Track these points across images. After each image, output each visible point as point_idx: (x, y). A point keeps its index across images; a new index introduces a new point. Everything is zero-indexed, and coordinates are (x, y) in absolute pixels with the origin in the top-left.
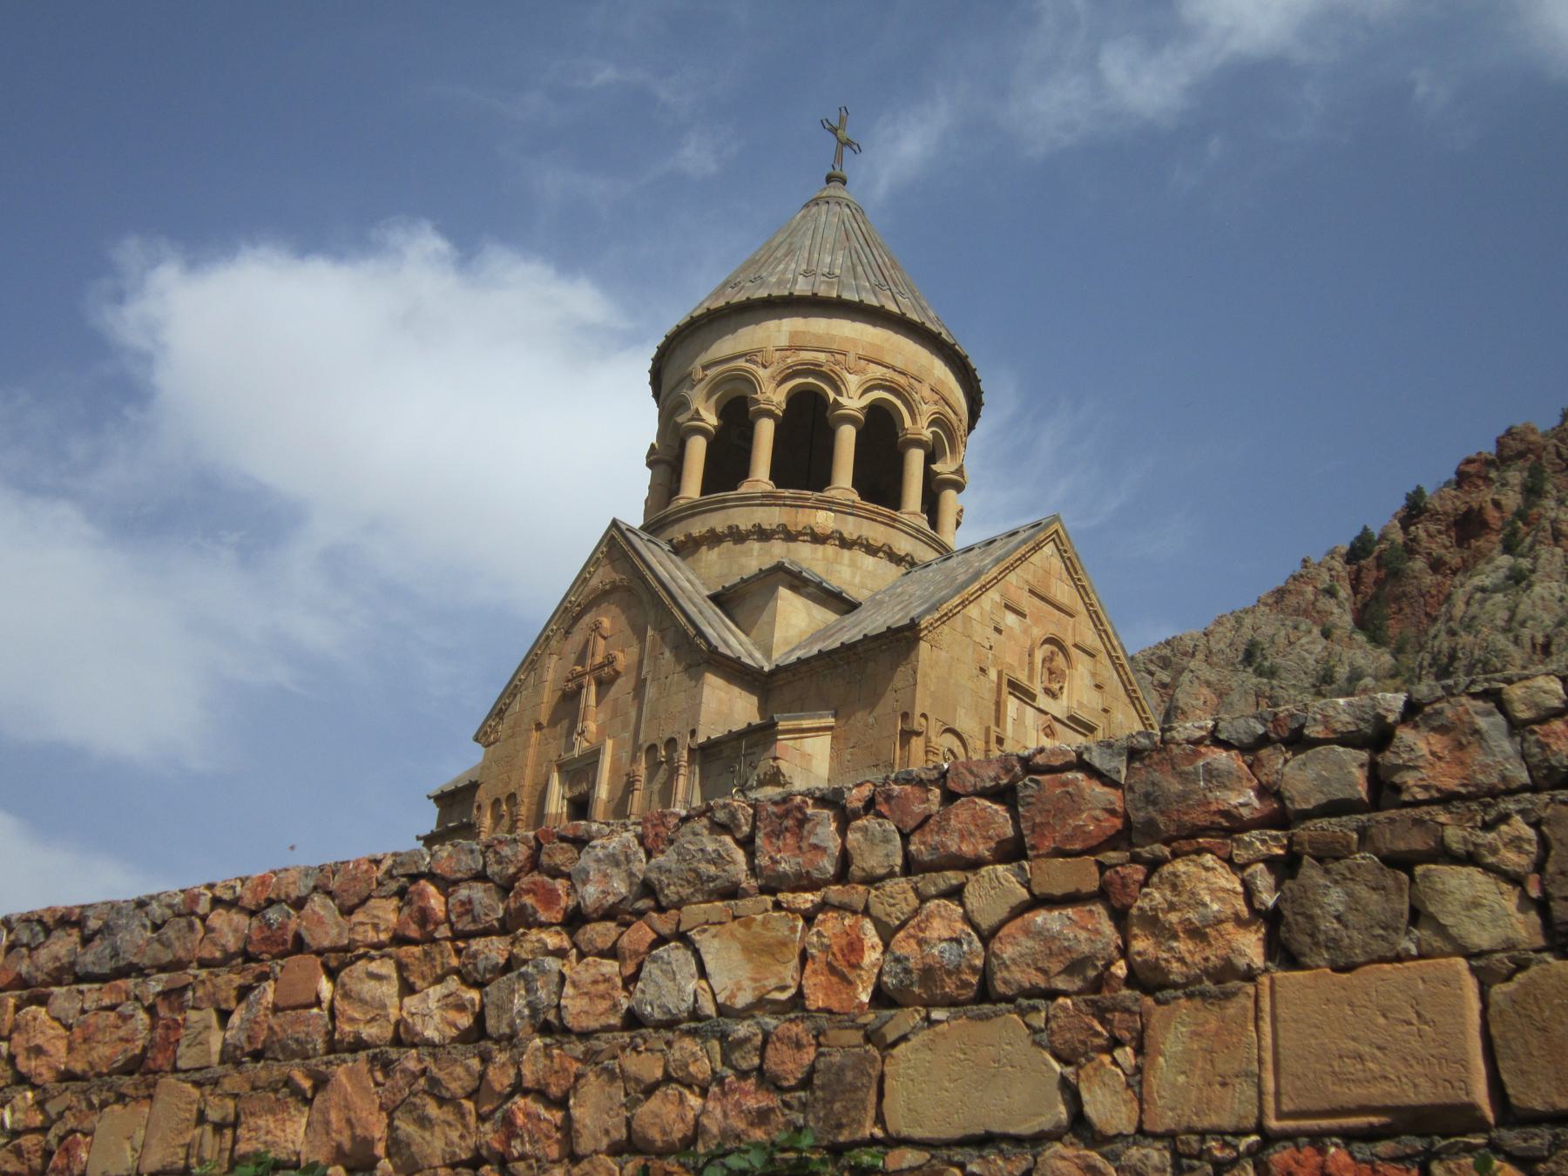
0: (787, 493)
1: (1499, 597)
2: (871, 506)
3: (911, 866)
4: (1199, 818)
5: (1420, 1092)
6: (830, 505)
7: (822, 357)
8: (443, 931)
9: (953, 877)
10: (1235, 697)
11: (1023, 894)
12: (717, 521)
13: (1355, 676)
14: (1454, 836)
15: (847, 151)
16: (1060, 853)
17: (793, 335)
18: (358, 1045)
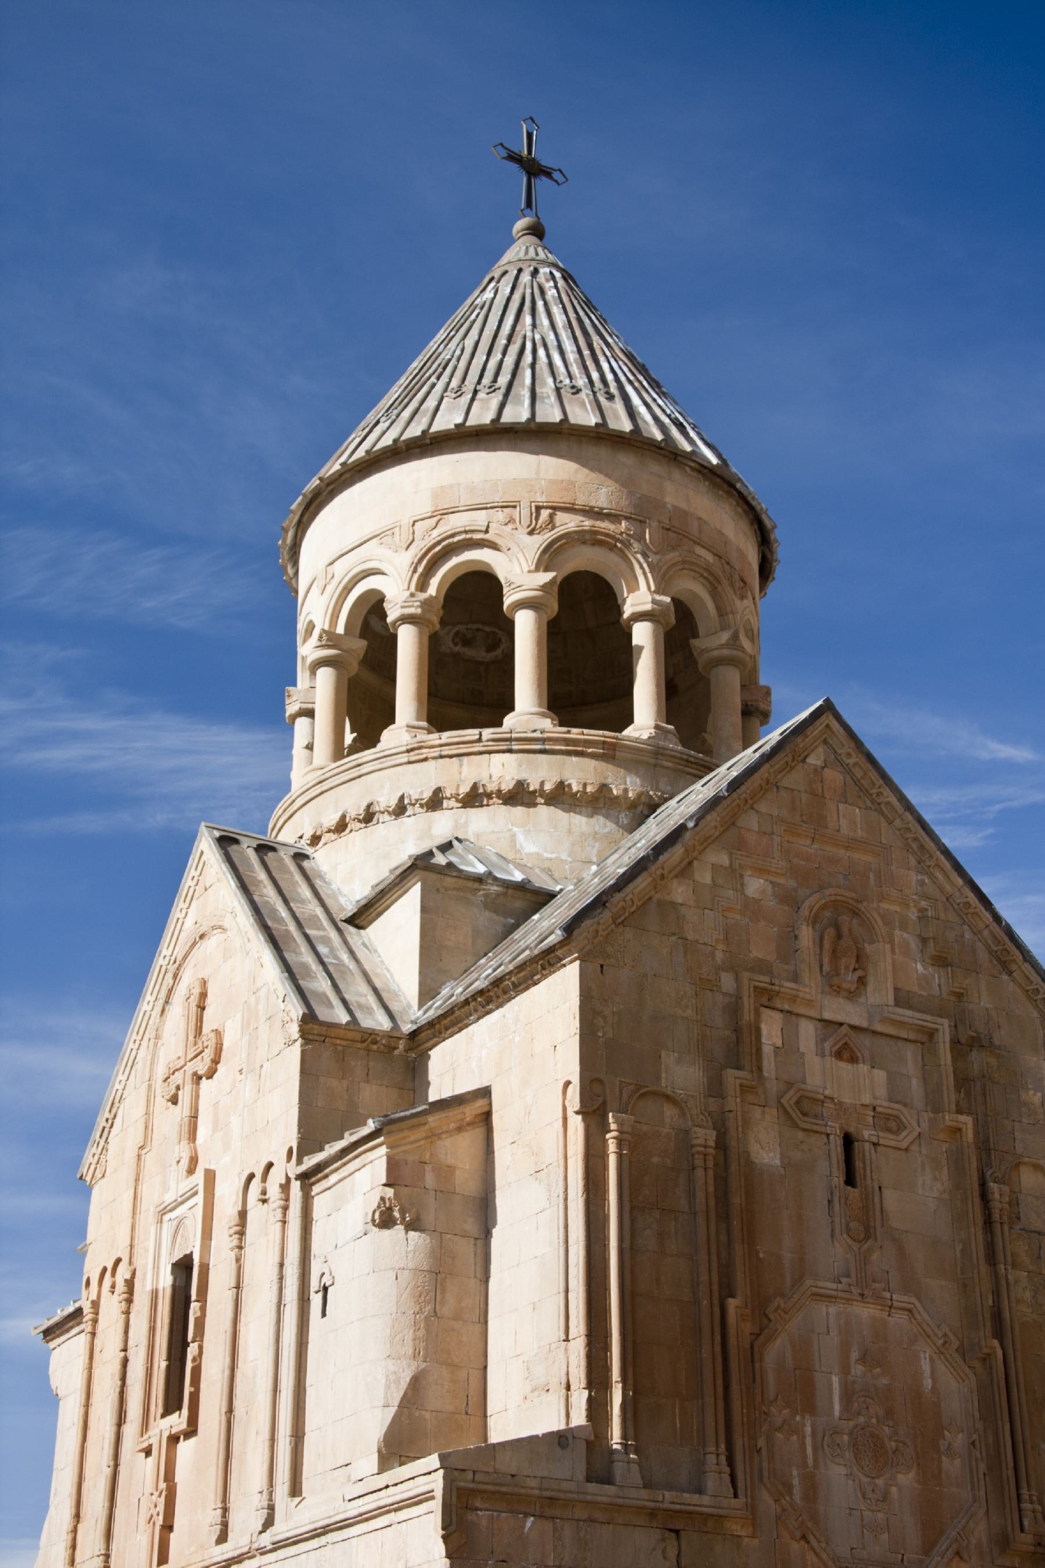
0: (447, 736)
2: (575, 733)
6: (507, 746)
7: (480, 519)
12: (350, 800)
15: (541, 184)
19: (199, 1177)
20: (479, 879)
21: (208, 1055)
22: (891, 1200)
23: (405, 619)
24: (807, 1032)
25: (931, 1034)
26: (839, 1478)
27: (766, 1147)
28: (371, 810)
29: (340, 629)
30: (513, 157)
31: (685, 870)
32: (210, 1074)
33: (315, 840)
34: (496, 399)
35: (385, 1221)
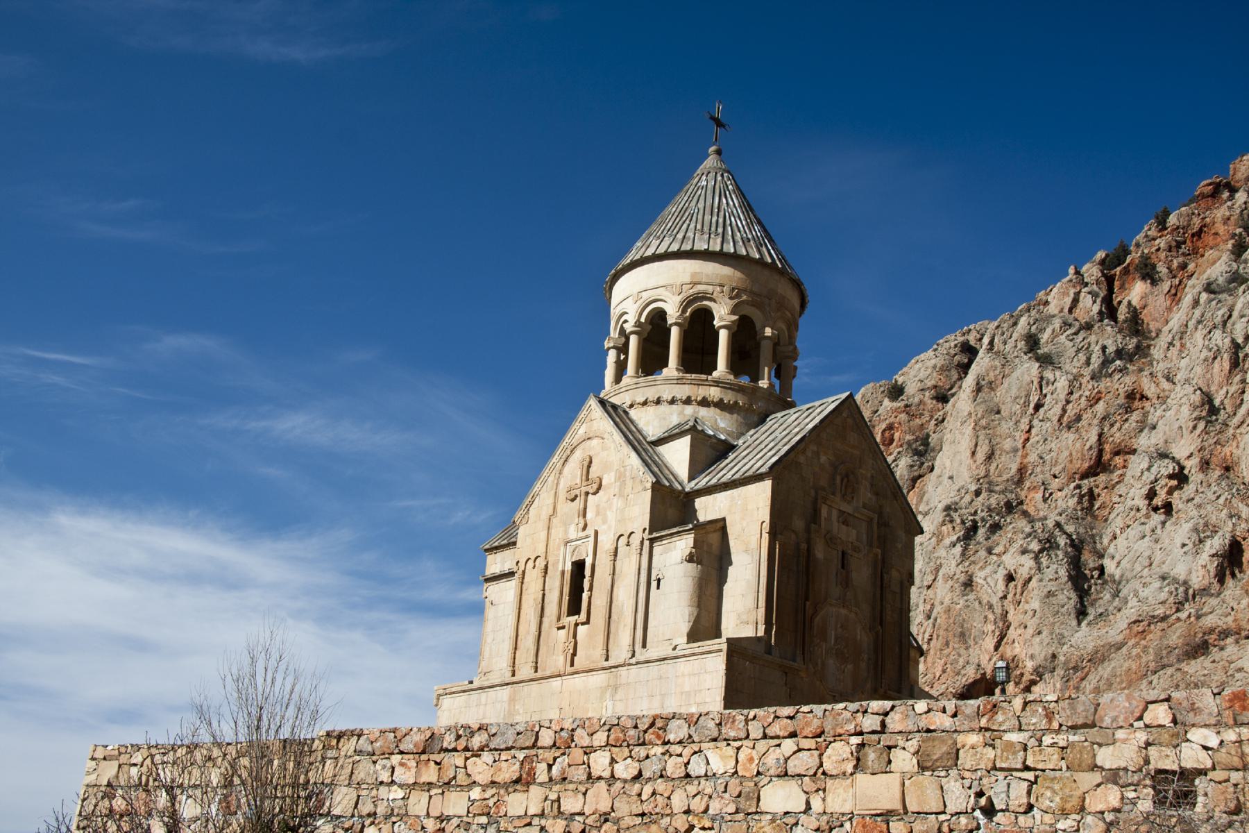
0: (693, 376)
1: (1223, 296)
3: (765, 736)
4: (841, 731)
5: (889, 807)
6: (717, 383)
7: (710, 289)
8: (625, 744)
9: (776, 742)
10: (1014, 375)
11: (796, 748)
12: (651, 394)
13: (1106, 362)
14: (901, 743)
16: (806, 737)
17: (694, 275)
18: (600, 778)
19: (590, 531)
20: (710, 436)
21: (595, 486)
22: (854, 575)
23: (676, 324)
24: (835, 513)
25: (872, 519)
26: (831, 663)
27: (820, 552)
28: (664, 403)
29: (643, 320)
30: (713, 118)
31: (804, 451)
32: (594, 494)
33: (631, 406)
34: (719, 240)
35: (690, 559)
